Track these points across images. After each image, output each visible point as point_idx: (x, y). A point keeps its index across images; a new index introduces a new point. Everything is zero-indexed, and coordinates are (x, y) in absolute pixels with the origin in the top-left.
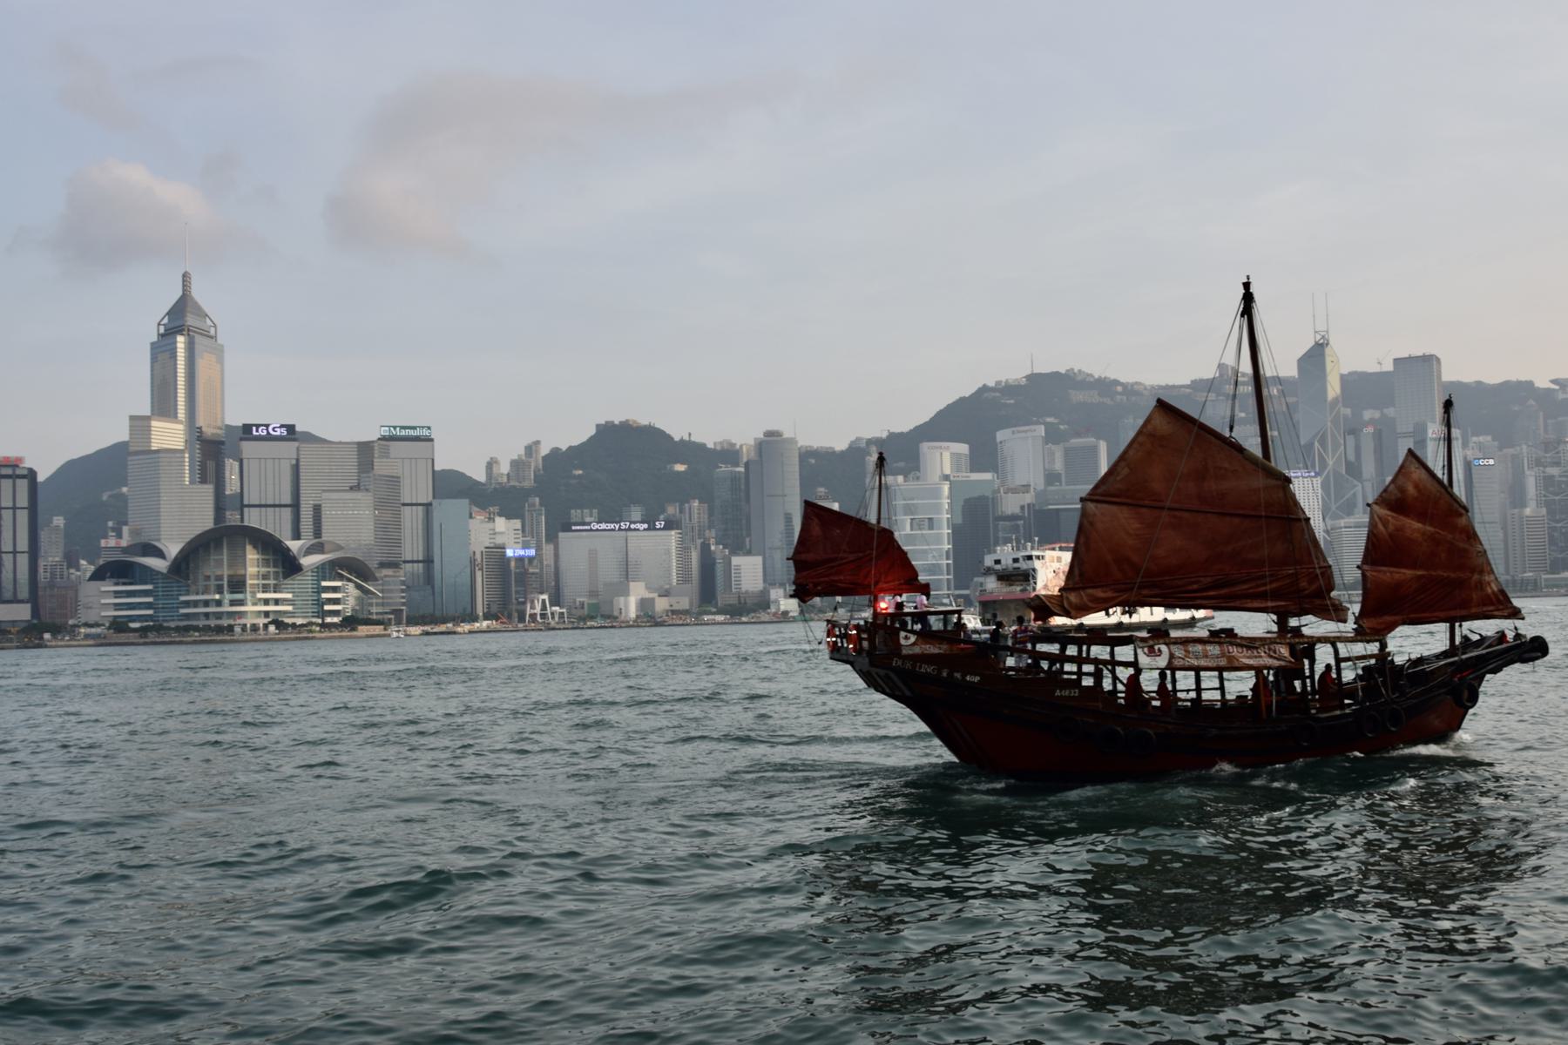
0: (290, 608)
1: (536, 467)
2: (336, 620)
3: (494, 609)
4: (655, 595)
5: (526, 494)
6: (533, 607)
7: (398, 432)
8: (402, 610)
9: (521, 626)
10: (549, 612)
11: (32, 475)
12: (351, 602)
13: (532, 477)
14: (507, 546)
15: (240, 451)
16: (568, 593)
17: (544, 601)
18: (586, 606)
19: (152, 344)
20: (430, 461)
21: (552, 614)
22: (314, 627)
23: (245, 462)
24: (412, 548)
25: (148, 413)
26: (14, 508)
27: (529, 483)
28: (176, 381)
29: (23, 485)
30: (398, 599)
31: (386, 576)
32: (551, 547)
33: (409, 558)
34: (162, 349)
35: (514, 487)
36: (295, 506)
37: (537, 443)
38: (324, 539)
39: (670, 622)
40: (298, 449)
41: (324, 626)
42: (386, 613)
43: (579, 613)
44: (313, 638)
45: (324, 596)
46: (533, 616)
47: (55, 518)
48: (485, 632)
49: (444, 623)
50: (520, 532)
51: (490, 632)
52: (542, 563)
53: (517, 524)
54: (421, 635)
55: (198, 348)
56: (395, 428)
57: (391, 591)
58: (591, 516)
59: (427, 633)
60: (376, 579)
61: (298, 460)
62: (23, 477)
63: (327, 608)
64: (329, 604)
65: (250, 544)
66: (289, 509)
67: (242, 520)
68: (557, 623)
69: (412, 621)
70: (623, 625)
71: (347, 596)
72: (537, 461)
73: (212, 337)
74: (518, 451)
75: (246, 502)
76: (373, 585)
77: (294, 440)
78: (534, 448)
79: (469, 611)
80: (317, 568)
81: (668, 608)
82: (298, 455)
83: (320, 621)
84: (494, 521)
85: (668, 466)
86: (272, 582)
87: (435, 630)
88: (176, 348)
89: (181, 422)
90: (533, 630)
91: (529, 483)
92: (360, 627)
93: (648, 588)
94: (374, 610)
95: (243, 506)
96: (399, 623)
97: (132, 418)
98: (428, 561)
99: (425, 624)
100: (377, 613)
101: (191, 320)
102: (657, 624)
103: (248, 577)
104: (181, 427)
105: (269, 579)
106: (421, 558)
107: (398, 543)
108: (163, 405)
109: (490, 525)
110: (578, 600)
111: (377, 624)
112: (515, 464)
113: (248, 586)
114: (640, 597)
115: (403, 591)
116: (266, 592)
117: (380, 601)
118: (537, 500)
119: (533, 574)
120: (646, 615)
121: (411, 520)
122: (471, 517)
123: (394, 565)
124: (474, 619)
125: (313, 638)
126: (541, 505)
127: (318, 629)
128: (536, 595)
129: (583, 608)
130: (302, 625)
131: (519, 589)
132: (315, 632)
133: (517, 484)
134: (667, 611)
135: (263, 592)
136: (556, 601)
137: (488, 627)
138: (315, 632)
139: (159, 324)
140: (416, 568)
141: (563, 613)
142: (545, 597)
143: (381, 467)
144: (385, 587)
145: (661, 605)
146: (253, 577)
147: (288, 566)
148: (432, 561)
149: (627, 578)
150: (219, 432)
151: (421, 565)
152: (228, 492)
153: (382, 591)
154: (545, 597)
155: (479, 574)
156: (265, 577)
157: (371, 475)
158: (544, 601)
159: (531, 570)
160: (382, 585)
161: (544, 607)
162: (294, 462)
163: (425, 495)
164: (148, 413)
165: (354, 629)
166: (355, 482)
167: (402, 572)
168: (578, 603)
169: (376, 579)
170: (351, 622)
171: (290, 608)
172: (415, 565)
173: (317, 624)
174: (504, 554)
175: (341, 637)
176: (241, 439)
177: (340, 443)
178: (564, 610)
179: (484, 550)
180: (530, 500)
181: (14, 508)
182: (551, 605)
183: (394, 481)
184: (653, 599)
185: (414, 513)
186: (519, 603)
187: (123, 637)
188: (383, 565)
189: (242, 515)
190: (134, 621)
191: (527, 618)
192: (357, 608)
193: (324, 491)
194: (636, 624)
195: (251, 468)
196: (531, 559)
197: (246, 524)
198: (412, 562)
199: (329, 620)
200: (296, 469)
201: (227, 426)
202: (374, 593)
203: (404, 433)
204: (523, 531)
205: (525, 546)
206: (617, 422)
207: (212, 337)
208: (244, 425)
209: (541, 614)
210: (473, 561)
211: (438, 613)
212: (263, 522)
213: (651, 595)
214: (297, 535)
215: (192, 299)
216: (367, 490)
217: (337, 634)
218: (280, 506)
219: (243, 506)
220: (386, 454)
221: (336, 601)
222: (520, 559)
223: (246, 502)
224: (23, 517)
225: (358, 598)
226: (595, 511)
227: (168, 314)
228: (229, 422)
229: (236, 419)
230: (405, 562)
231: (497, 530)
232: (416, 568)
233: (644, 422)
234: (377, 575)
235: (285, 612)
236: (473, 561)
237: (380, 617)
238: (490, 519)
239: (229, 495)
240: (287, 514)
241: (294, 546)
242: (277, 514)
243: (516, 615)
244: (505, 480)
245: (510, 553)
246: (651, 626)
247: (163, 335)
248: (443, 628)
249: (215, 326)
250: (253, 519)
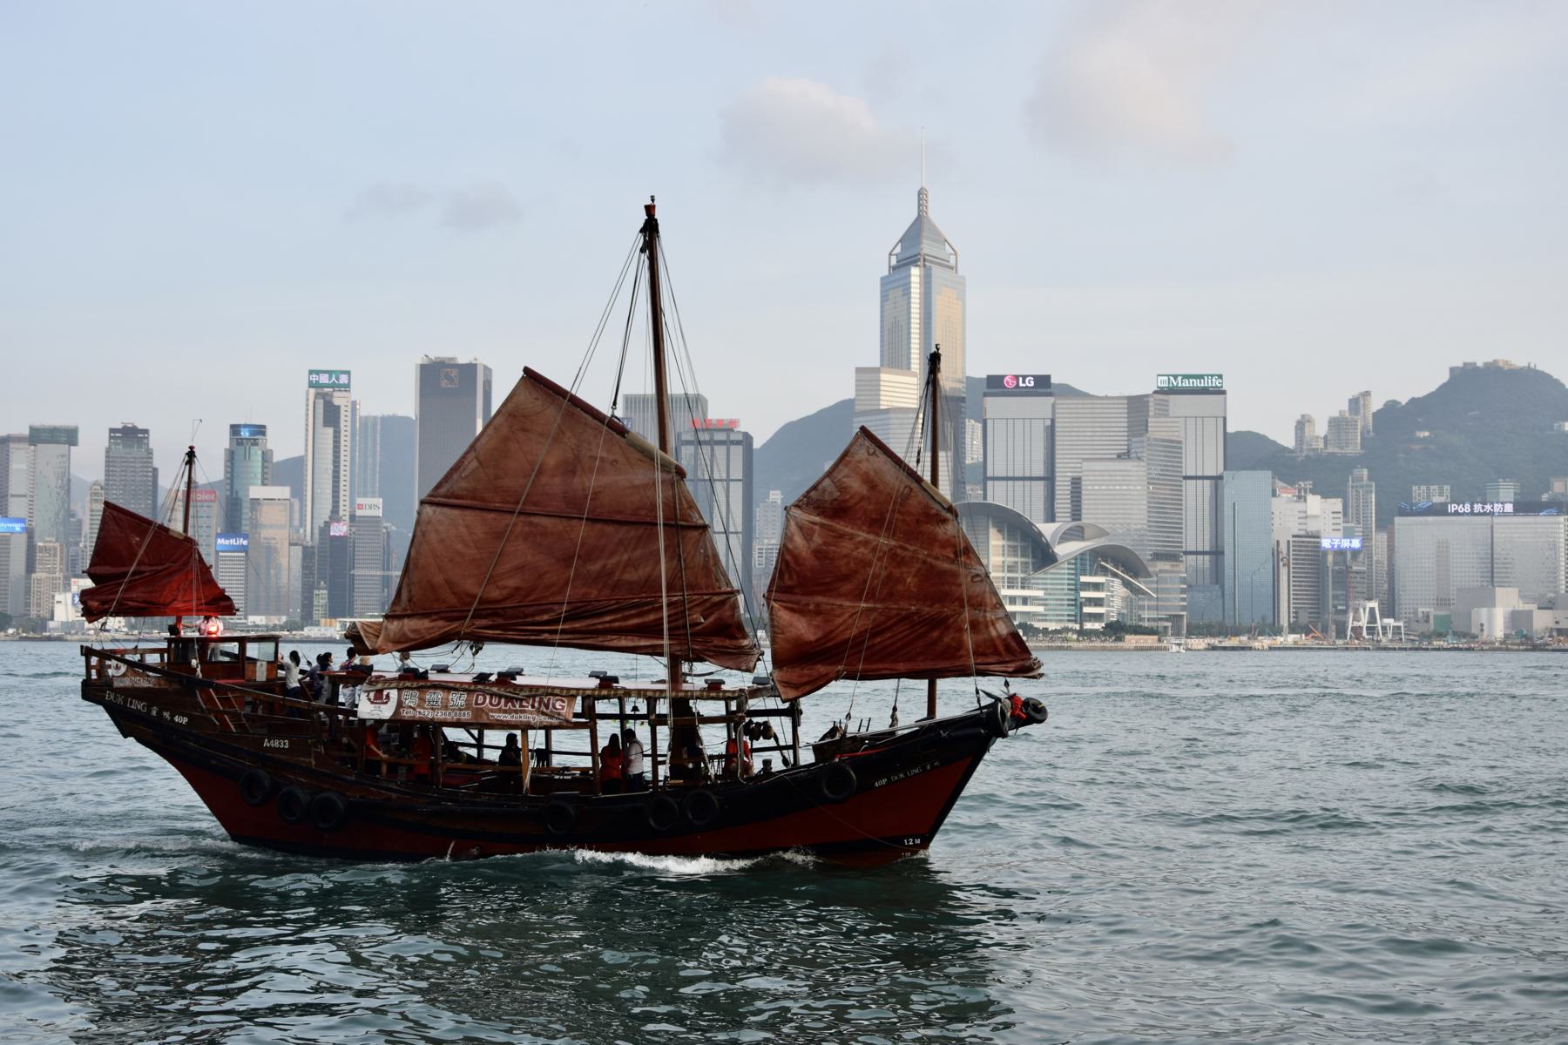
0: (1041, 609)
1: (1364, 427)
2: (1097, 626)
3: (1304, 618)
4: (1533, 607)
5: (1349, 464)
6: (1356, 619)
7: (1180, 383)
8: (1182, 616)
9: (1340, 642)
10: (1379, 625)
11: (748, 439)
12: (1117, 603)
13: (1359, 441)
14: (1322, 535)
15: (983, 409)
16: (1406, 600)
17: (1372, 610)
18: (1431, 618)
19: (882, 279)
20: (1221, 421)
21: (1384, 628)
22: (1070, 635)
23: (989, 423)
24: (1196, 535)
25: (877, 364)
26: (728, 480)
27: (1354, 448)
28: (909, 323)
29: (737, 452)
30: (1176, 601)
31: (1160, 571)
32: (1384, 536)
33: (1191, 548)
34: (893, 284)
35: (1333, 454)
36: (1050, 479)
37: (1367, 394)
38: (1083, 521)
39: (1555, 646)
40: (1053, 406)
41: (1082, 633)
42: (1161, 619)
43: (1423, 628)
44: (1069, 648)
45: (1084, 594)
46: (1357, 631)
47: (771, 492)
48: (1291, 649)
49: (1236, 634)
50: (1341, 515)
51: (1298, 649)
52: (1370, 557)
53: (1337, 504)
54: (1206, 649)
55: (935, 281)
56: (1175, 377)
57: (1167, 591)
58: (1441, 494)
59: (1214, 648)
60: (1149, 575)
61: (1053, 421)
62: (738, 443)
63: (1086, 610)
64: (1090, 605)
65: (994, 526)
66: (1041, 483)
67: (985, 497)
68: (1391, 641)
69: (1194, 631)
70: (1485, 648)
71: (1113, 597)
72: (1365, 417)
73: (952, 268)
74: (1340, 406)
75: (989, 474)
76: (1145, 583)
77: (1050, 395)
78: (1362, 402)
79: (1270, 620)
80: (1076, 558)
81: (1552, 625)
82: (1054, 413)
83: (1077, 627)
84: (1305, 500)
85: (1556, 425)
86: (1020, 575)
87: (1223, 645)
88: (910, 283)
89: (914, 375)
90: (1356, 649)
91: (1354, 448)
92: (1128, 637)
93: (1523, 597)
94: (1146, 614)
95: (986, 479)
96: (1177, 634)
97: (859, 370)
98: (1217, 553)
99: (1213, 635)
100: (1149, 619)
101: (927, 248)
102: (1535, 648)
103: (991, 567)
104: (915, 380)
105: (1017, 572)
106: (1207, 549)
107: (1177, 527)
108: (894, 356)
109: (1301, 506)
110: (1420, 610)
111: (1149, 634)
112: (1336, 424)
114: (1511, 609)
115: (1183, 591)
116: (1013, 587)
117: (1154, 603)
118: (1365, 472)
119: (1357, 572)
120: (1519, 634)
121: (1196, 496)
122: (1274, 494)
123: (1172, 557)
124: (1276, 631)
125: (1069, 648)
126: (1370, 479)
127: (1075, 637)
128: (1362, 602)
129: (1427, 621)
130: (1056, 632)
131: (1339, 592)
132: (1072, 641)
133: (1336, 450)
134: (1552, 630)
135: (1009, 587)
136: (1389, 610)
137: (1295, 642)
138: (1072, 641)
139: (890, 254)
140: (1200, 563)
141: (1399, 628)
142: (1374, 604)
143: (1158, 428)
144: (1159, 586)
145: (1542, 621)
146: (996, 568)
147: (1042, 556)
148: (1222, 553)
149: (1492, 581)
150: (960, 386)
151: (1207, 557)
152: (968, 461)
153: (1156, 591)
154: (1374, 604)
155: (1283, 571)
156: (1011, 569)
157: (1145, 439)
158: (1372, 610)
159: (1355, 568)
160: (1157, 583)
161: (1372, 619)
162: (1048, 423)
163: (1213, 466)
164: (877, 364)
165: (1119, 639)
166: (1123, 448)
167: (1182, 567)
168: (1420, 615)
169: (1149, 575)
170: (1116, 630)
171: (1041, 609)
172: (1200, 557)
173: (1074, 631)
174: (1318, 546)
175: (1104, 649)
176: (985, 395)
177: (1106, 398)
178: (1401, 624)
179: (1291, 539)
180: (1356, 472)
181: (728, 480)
182: (1383, 616)
183: (1173, 448)
184: (1530, 613)
185: (1200, 489)
186: (1338, 612)
188: (1158, 557)
189: (985, 490)
191: (1349, 633)
192: (1125, 611)
193: (1085, 460)
194: (1505, 646)
195: (997, 431)
196: (1355, 553)
197: (989, 501)
198: (1196, 553)
199: (1088, 626)
200: (1051, 431)
201: (968, 378)
202: (1145, 593)
203: (1187, 384)
204: (1345, 514)
205: (1348, 534)
206: (1480, 364)
207: (952, 268)
208: (988, 376)
209: (1368, 628)
210: (1276, 553)
211: (1228, 622)
212: (1010, 498)
213: (1527, 607)
214: (1051, 517)
215: (930, 221)
216: (1139, 458)
217: (1098, 644)
218: (1031, 479)
219: (986, 479)
220: (1164, 411)
221: (1098, 602)
222: (1340, 553)
223: (989, 474)
224: (737, 490)
225: (1125, 599)
226: (1447, 488)
227: (900, 241)
228: (968, 374)
229: (979, 369)
230: (1186, 553)
231: (1309, 513)
232: (1200, 563)
233: (1519, 361)
234: (1150, 569)
235: (1035, 614)
236: (1276, 553)
237: (1153, 624)
238: (1299, 497)
239: (971, 465)
240: (1039, 488)
241: (1047, 530)
242: (1027, 489)
243: (1334, 627)
244: (1321, 445)
245: (1326, 543)
246: (1526, 650)
247: (895, 268)
248: (1234, 642)
249: (956, 254)
250: (998, 495)
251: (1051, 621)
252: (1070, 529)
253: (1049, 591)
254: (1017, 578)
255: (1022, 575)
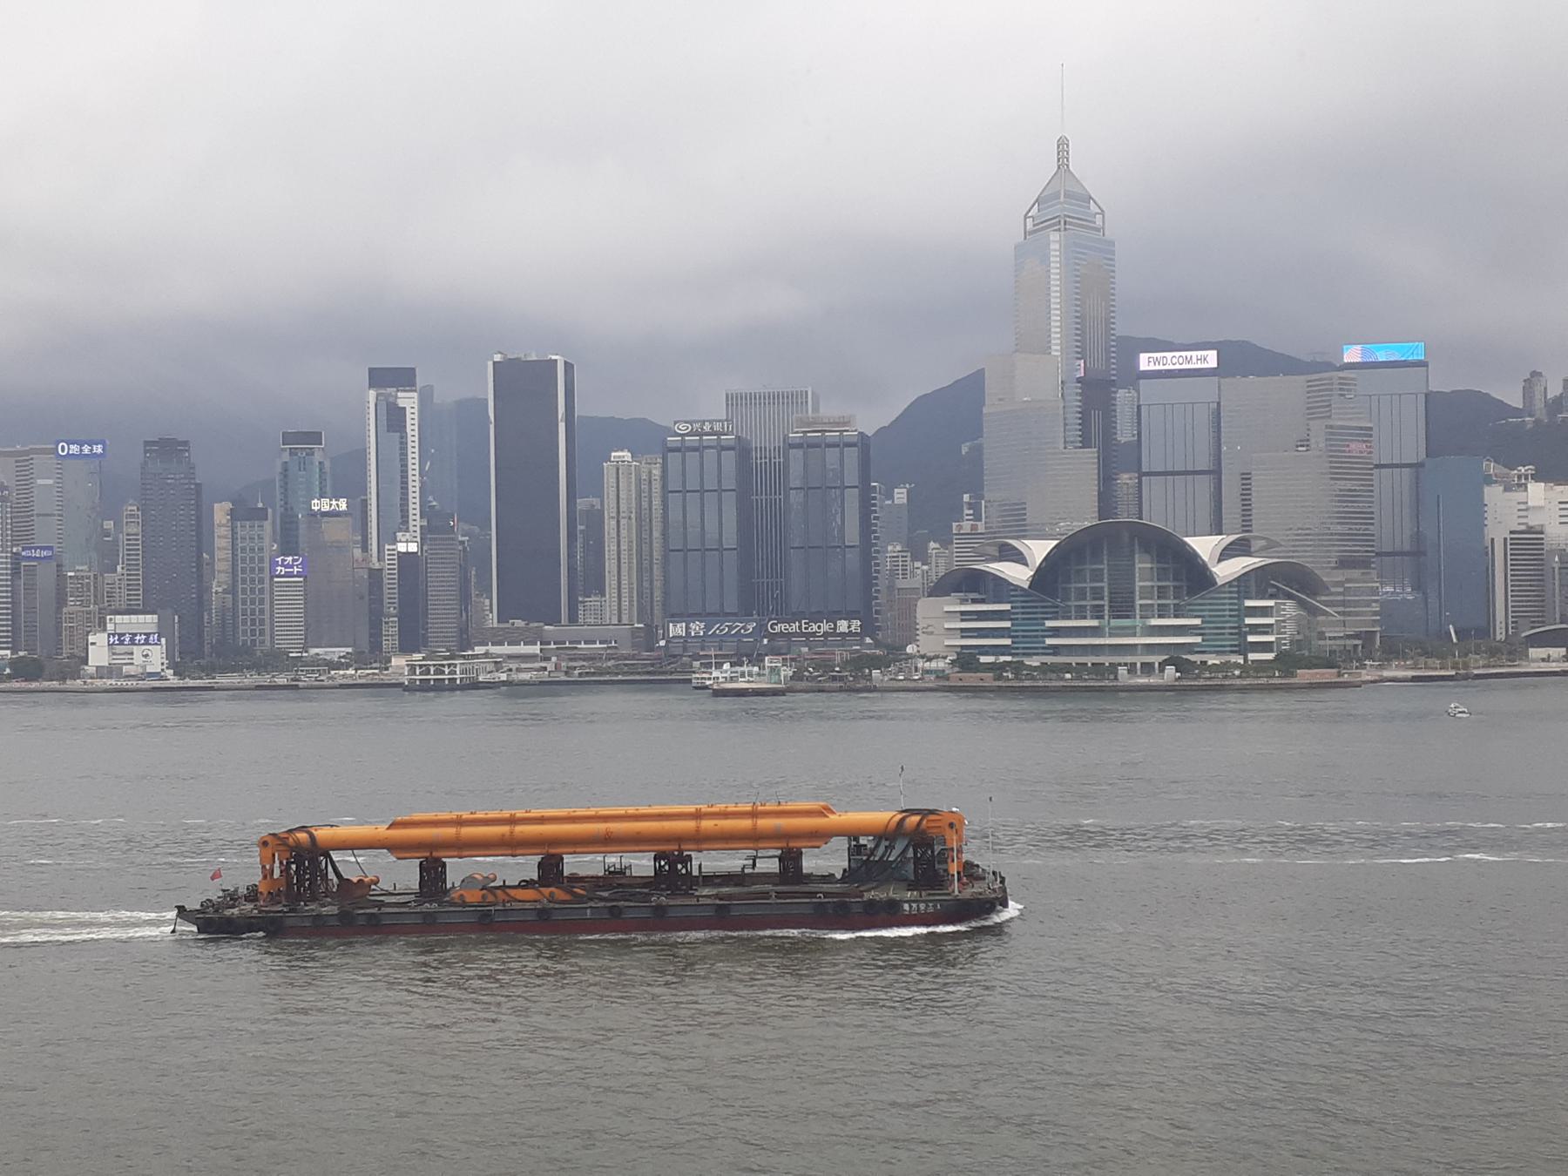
12: (1290, 629)
69: (1391, 652)
113: (1138, 607)
187: (971, 679)
190: (986, 654)
251: (1211, 653)
252: (1231, 544)
253: (1208, 619)
254: (1169, 605)
255: (1176, 601)
